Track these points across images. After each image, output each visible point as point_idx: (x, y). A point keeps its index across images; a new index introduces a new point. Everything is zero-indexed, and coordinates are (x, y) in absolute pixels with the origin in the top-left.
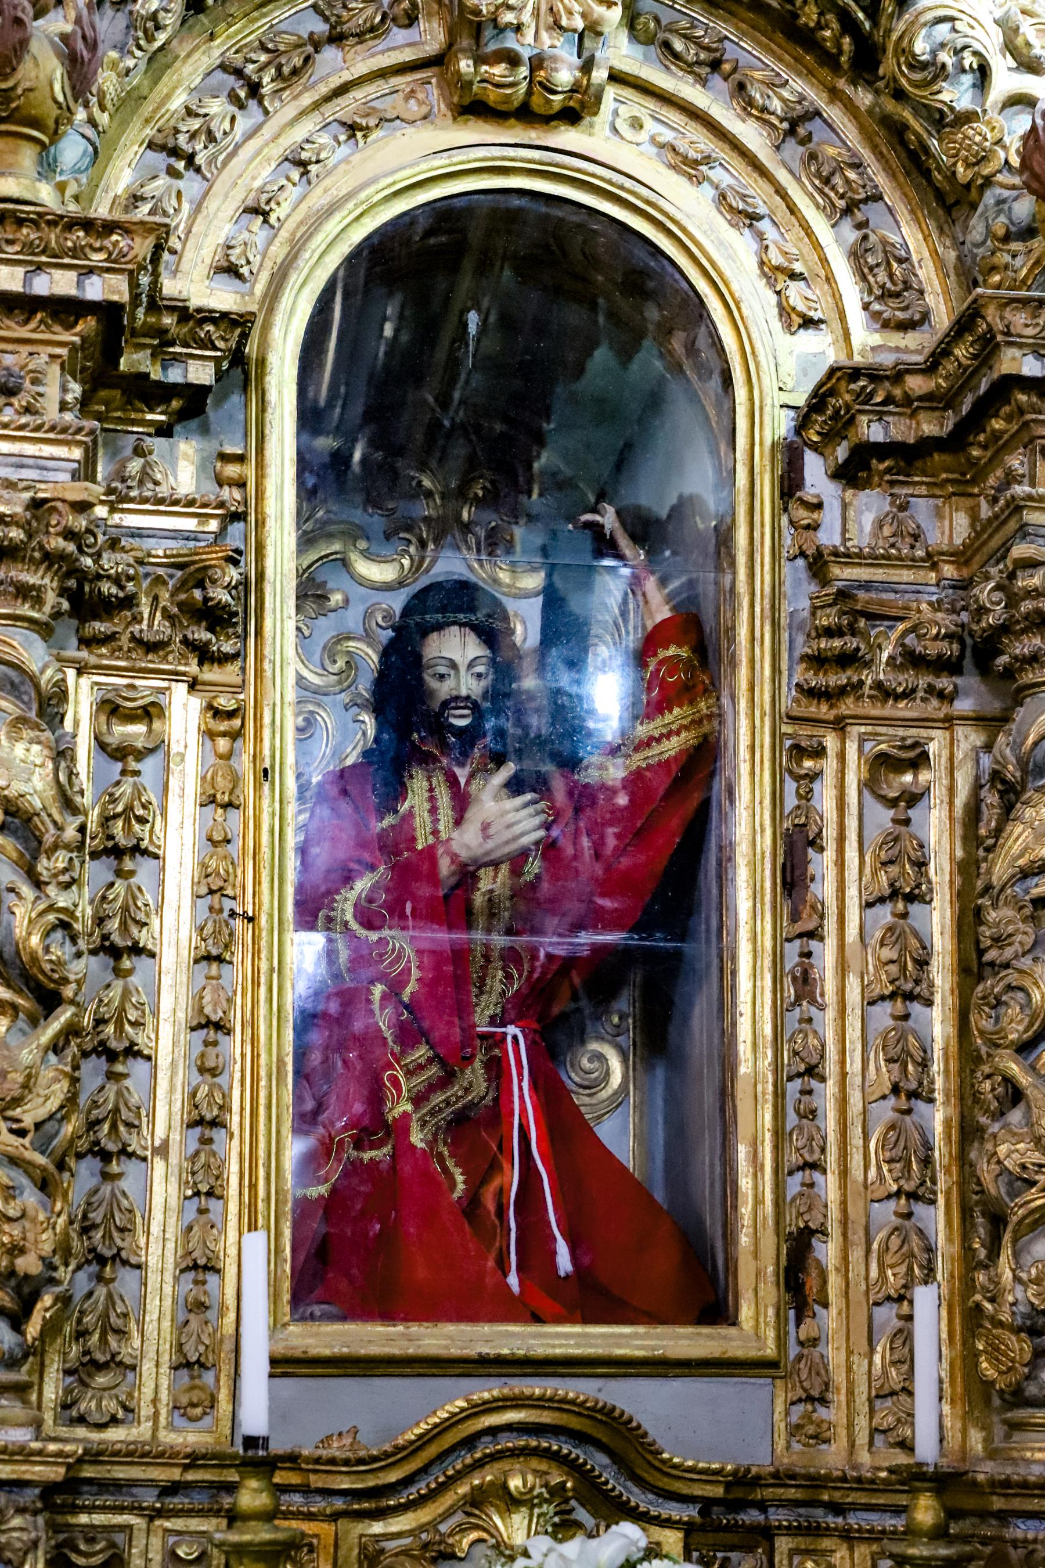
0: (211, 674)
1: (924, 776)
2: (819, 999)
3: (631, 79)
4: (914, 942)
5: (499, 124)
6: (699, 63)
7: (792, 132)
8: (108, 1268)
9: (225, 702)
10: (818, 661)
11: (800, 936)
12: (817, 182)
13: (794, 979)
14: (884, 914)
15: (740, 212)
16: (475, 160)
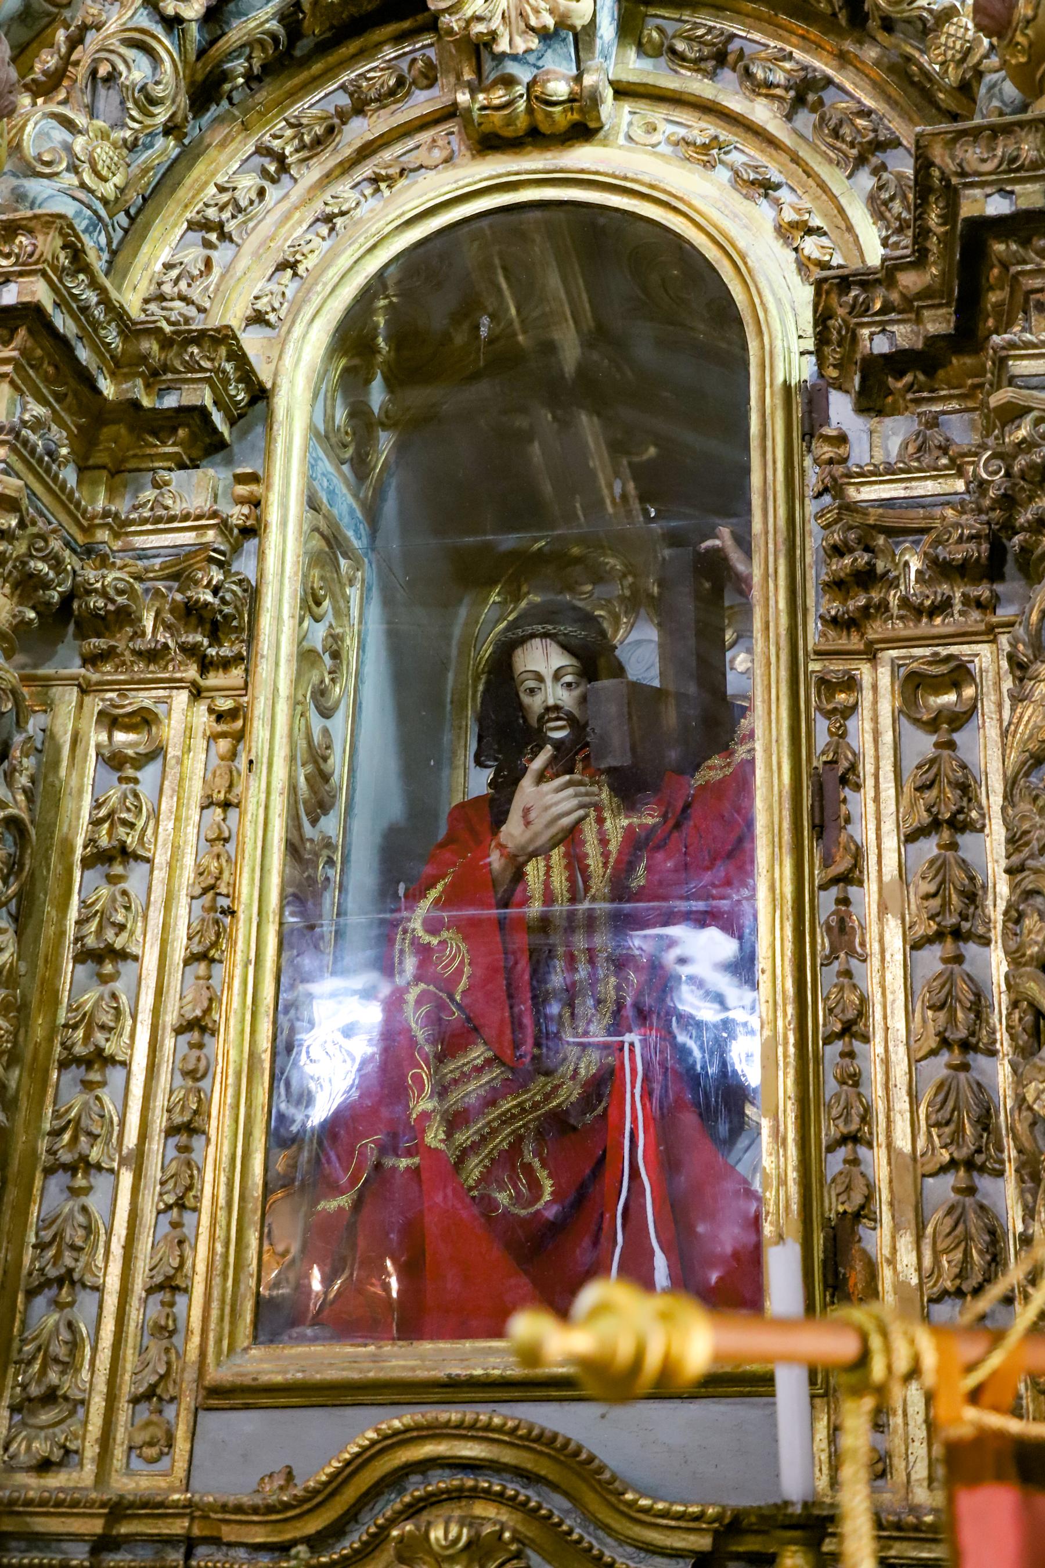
0: (214, 679)
1: (969, 692)
2: (859, 949)
3: (641, 90)
4: (958, 874)
5: (516, 153)
6: (702, 59)
7: (800, 101)
8: (64, 1291)
9: (225, 704)
10: (838, 586)
11: (836, 881)
12: (829, 140)
13: (829, 929)
14: (929, 847)
15: (753, 183)
16: (481, 181)
